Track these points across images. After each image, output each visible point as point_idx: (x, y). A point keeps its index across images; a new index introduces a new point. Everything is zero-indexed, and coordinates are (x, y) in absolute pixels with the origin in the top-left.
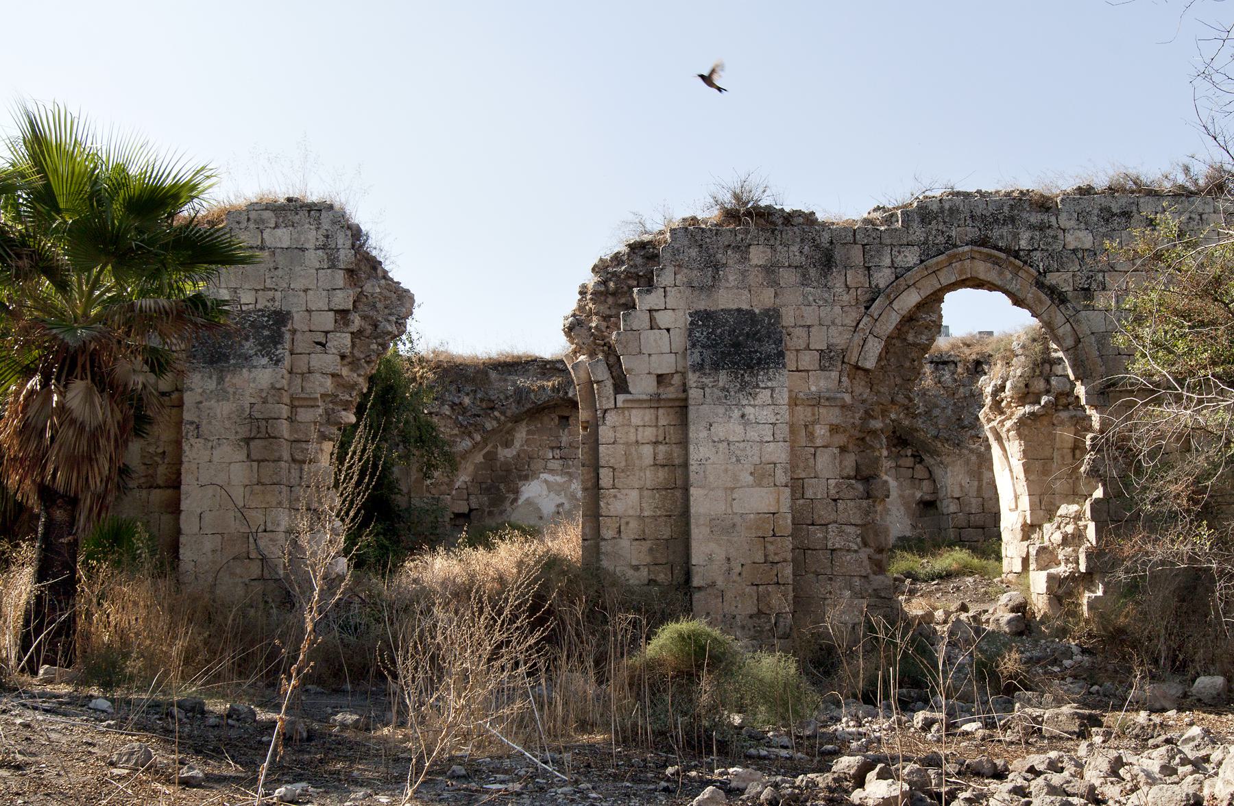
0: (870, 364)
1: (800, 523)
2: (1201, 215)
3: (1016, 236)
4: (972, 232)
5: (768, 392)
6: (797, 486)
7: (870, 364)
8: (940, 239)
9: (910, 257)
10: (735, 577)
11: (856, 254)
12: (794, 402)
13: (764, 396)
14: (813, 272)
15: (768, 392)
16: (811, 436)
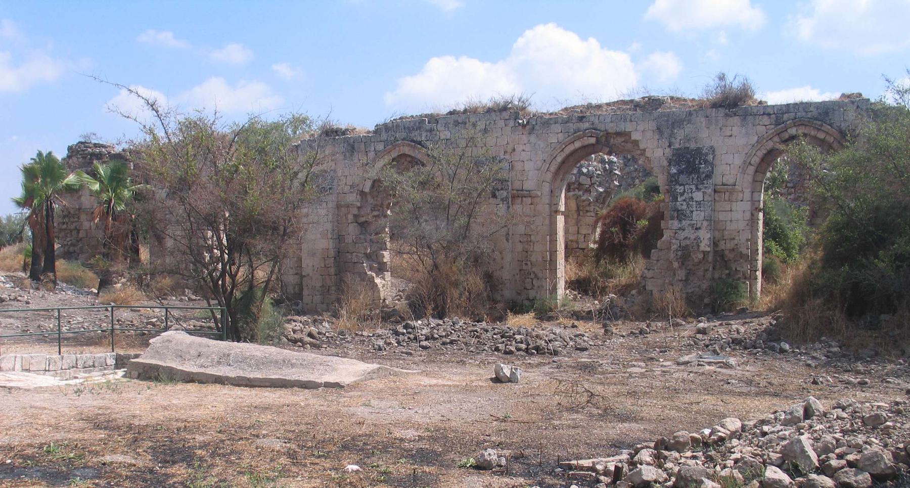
0: (367, 190)
1: (339, 253)
2: (495, 121)
3: (421, 135)
4: (404, 135)
5: (325, 203)
6: (340, 238)
7: (367, 190)
8: (393, 138)
9: (380, 147)
10: (315, 273)
11: (362, 146)
12: (338, 207)
13: (324, 205)
14: (347, 154)
15: (325, 203)
16: (347, 219)
